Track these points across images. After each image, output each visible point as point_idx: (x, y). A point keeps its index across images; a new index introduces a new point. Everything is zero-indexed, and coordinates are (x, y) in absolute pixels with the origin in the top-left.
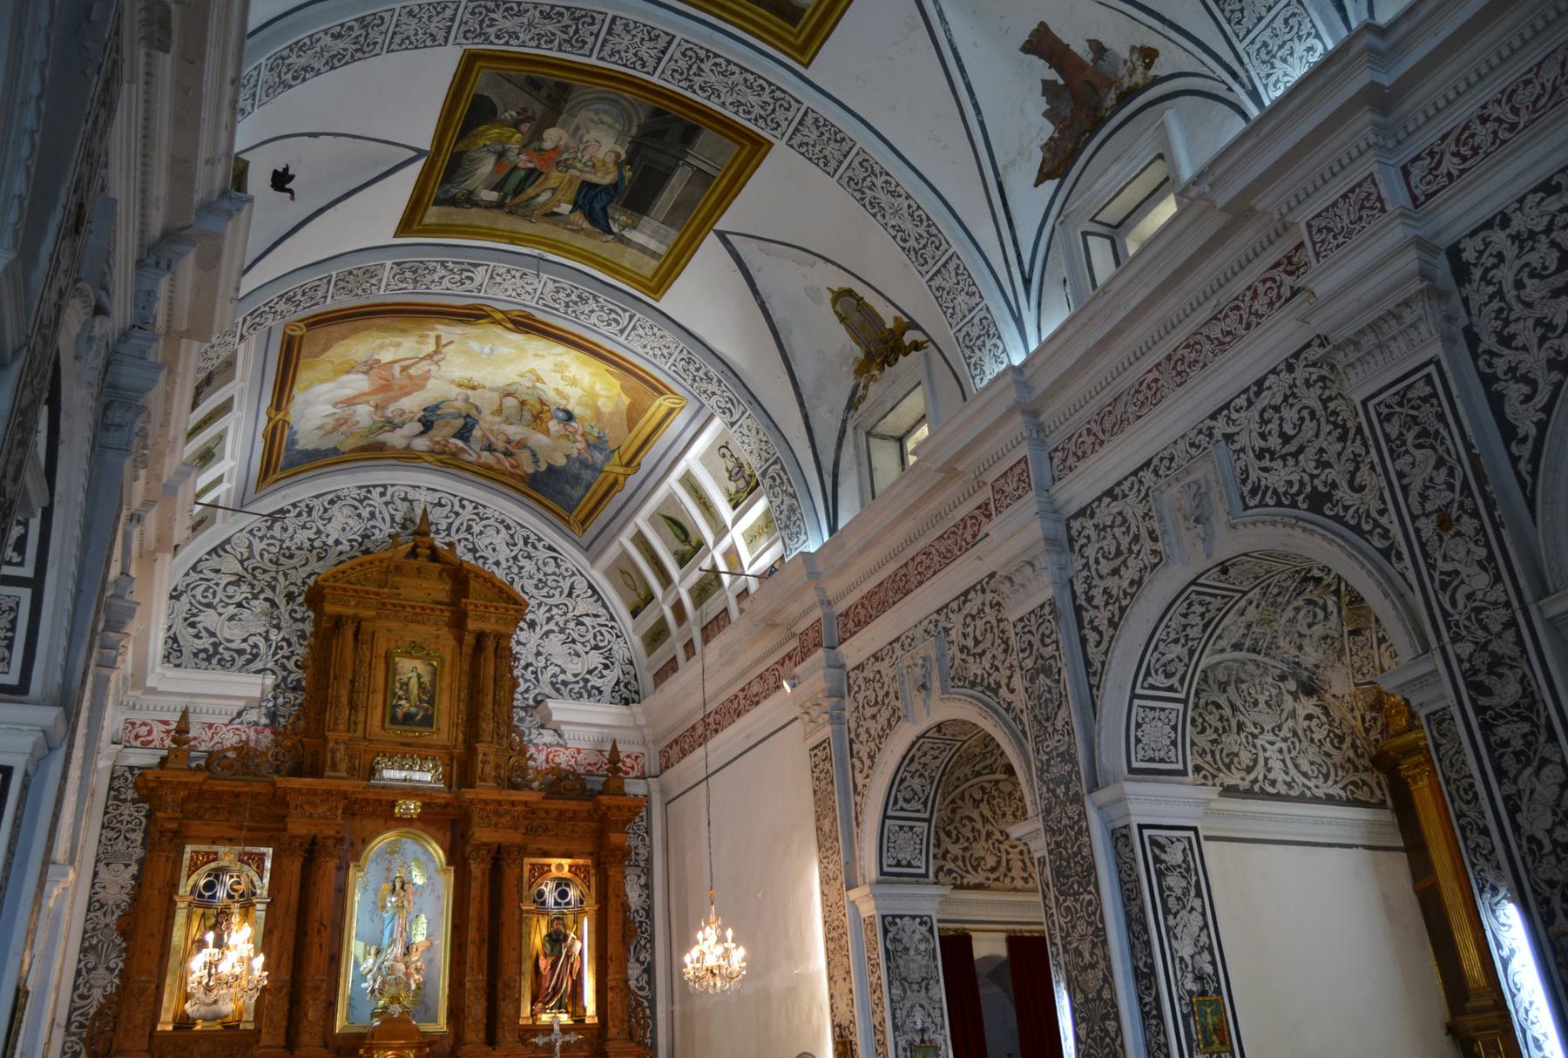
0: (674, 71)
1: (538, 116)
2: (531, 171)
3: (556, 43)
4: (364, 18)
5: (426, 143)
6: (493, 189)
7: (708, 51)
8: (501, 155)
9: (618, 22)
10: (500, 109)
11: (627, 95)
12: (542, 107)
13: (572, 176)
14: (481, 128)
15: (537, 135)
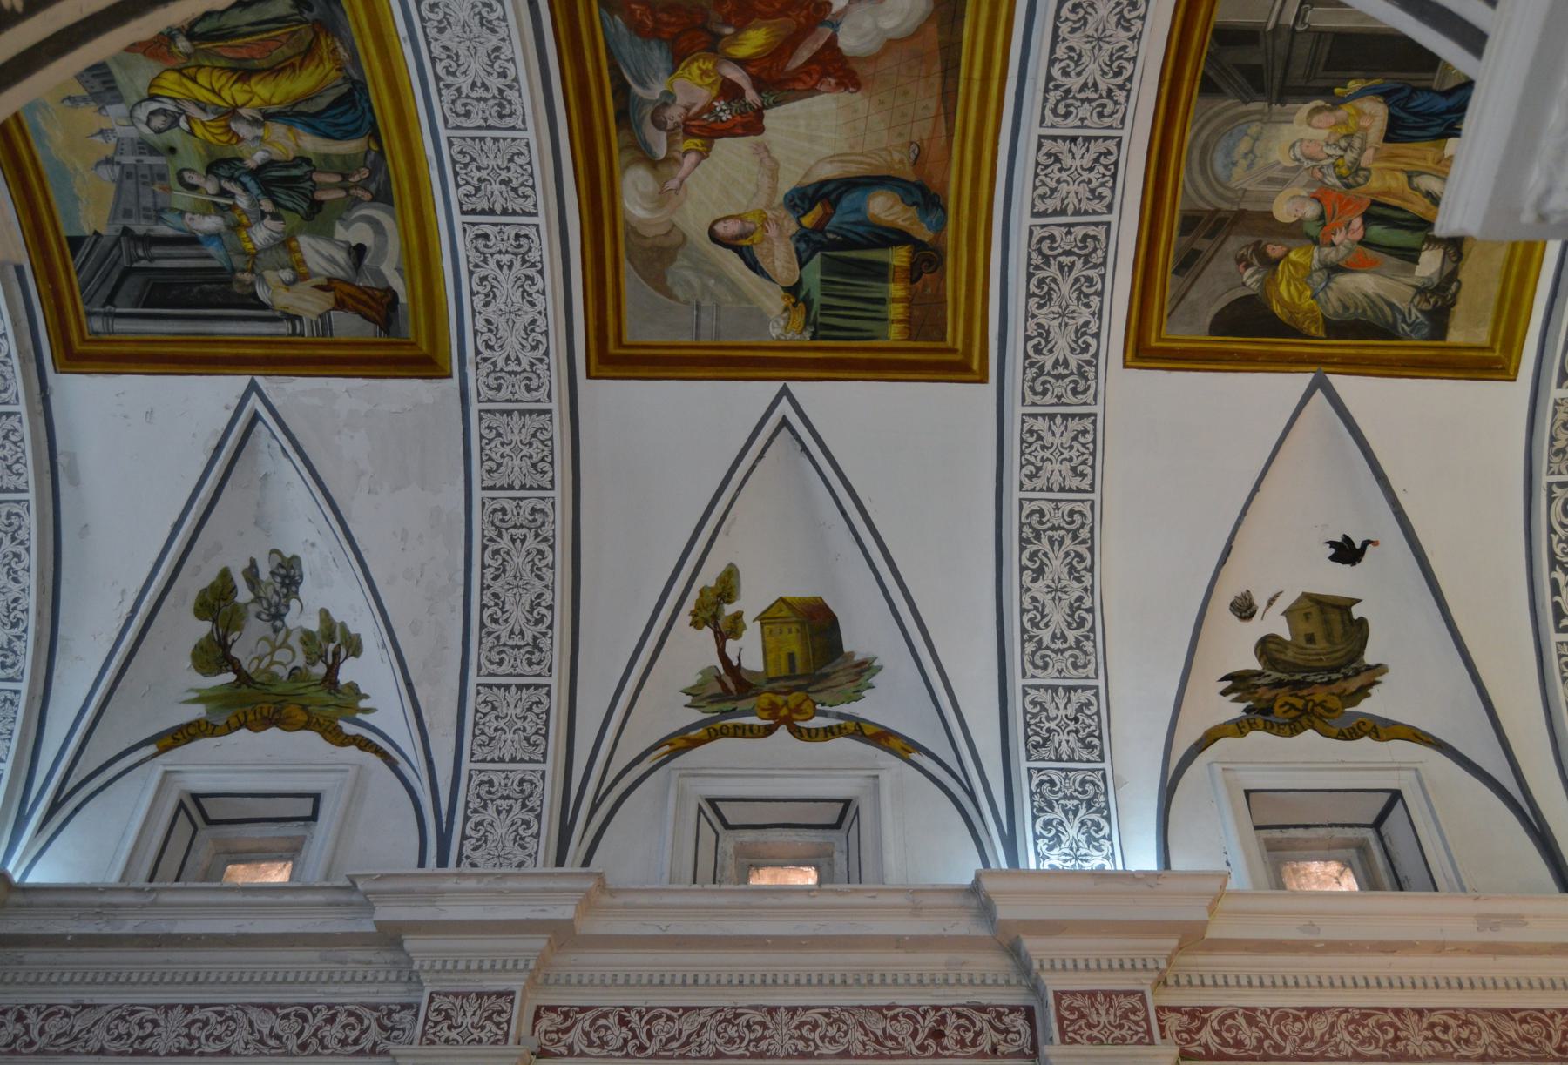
0: (1101, 115)
1: (1250, 240)
2: (1368, 218)
3: (1091, 273)
4: (1022, 539)
5: (1302, 380)
6: (1415, 261)
7: (1047, 90)
8: (1334, 269)
9: (1040, 207)
10: (1240, 293)
11: (1188, 136)
12: (1231, 238)
13: (1375, 159)
14: (1277, 309)
15: (1295, 232)
